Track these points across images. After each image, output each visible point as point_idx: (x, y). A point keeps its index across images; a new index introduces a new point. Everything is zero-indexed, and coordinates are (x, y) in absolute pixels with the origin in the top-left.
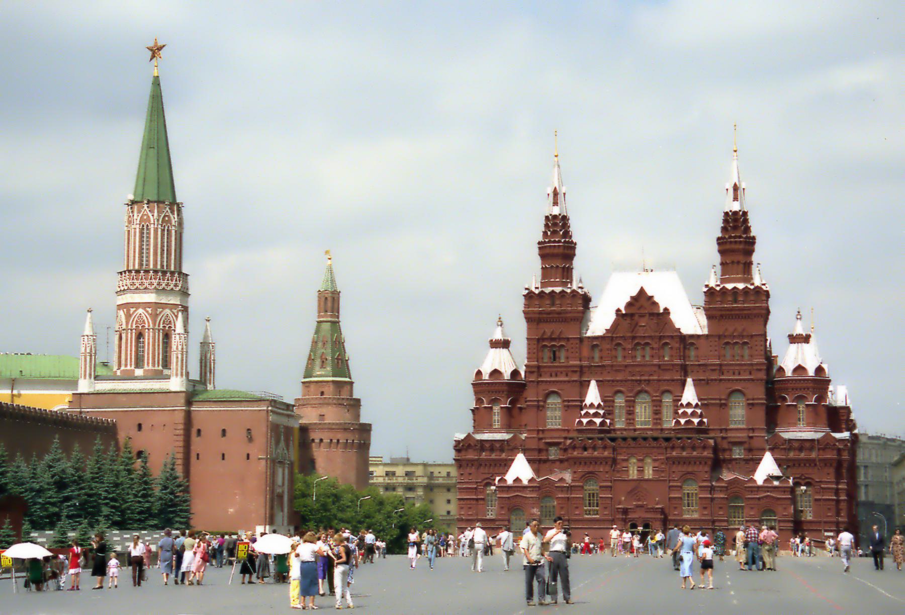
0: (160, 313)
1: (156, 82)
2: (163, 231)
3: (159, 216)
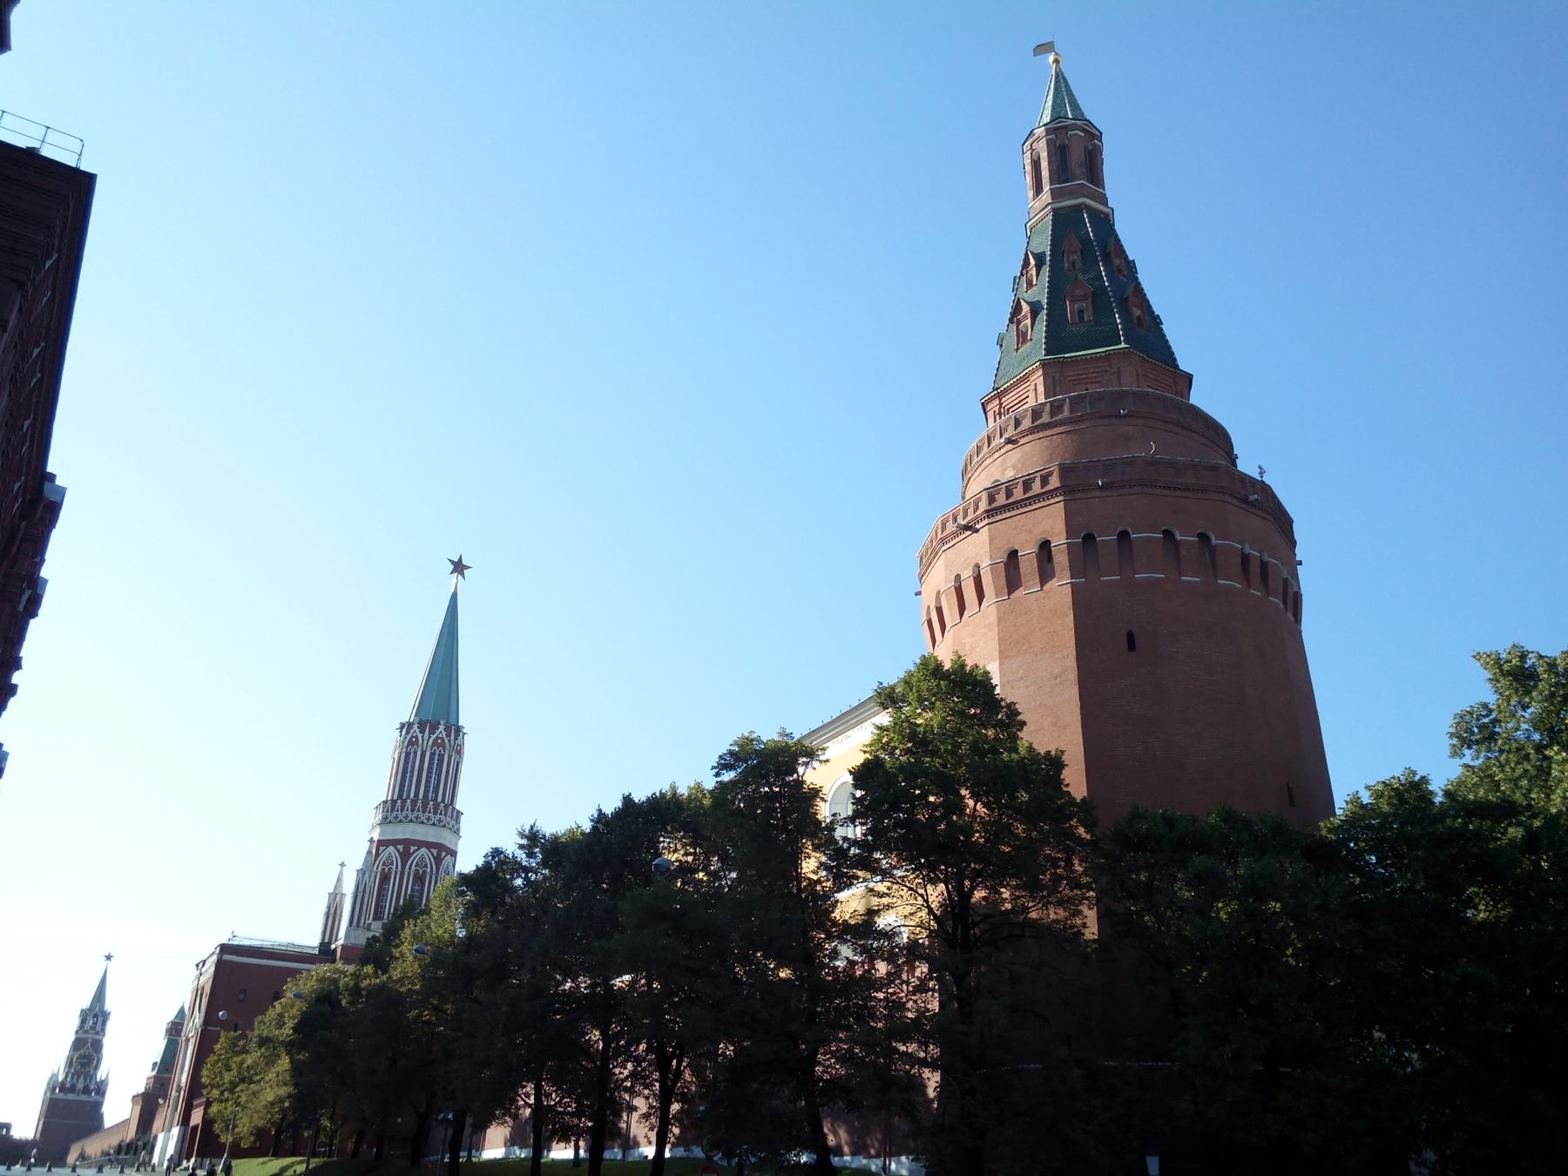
0: (414, 852)
1: (454, 598)
2: (433, 755)
3: (430, 737)
